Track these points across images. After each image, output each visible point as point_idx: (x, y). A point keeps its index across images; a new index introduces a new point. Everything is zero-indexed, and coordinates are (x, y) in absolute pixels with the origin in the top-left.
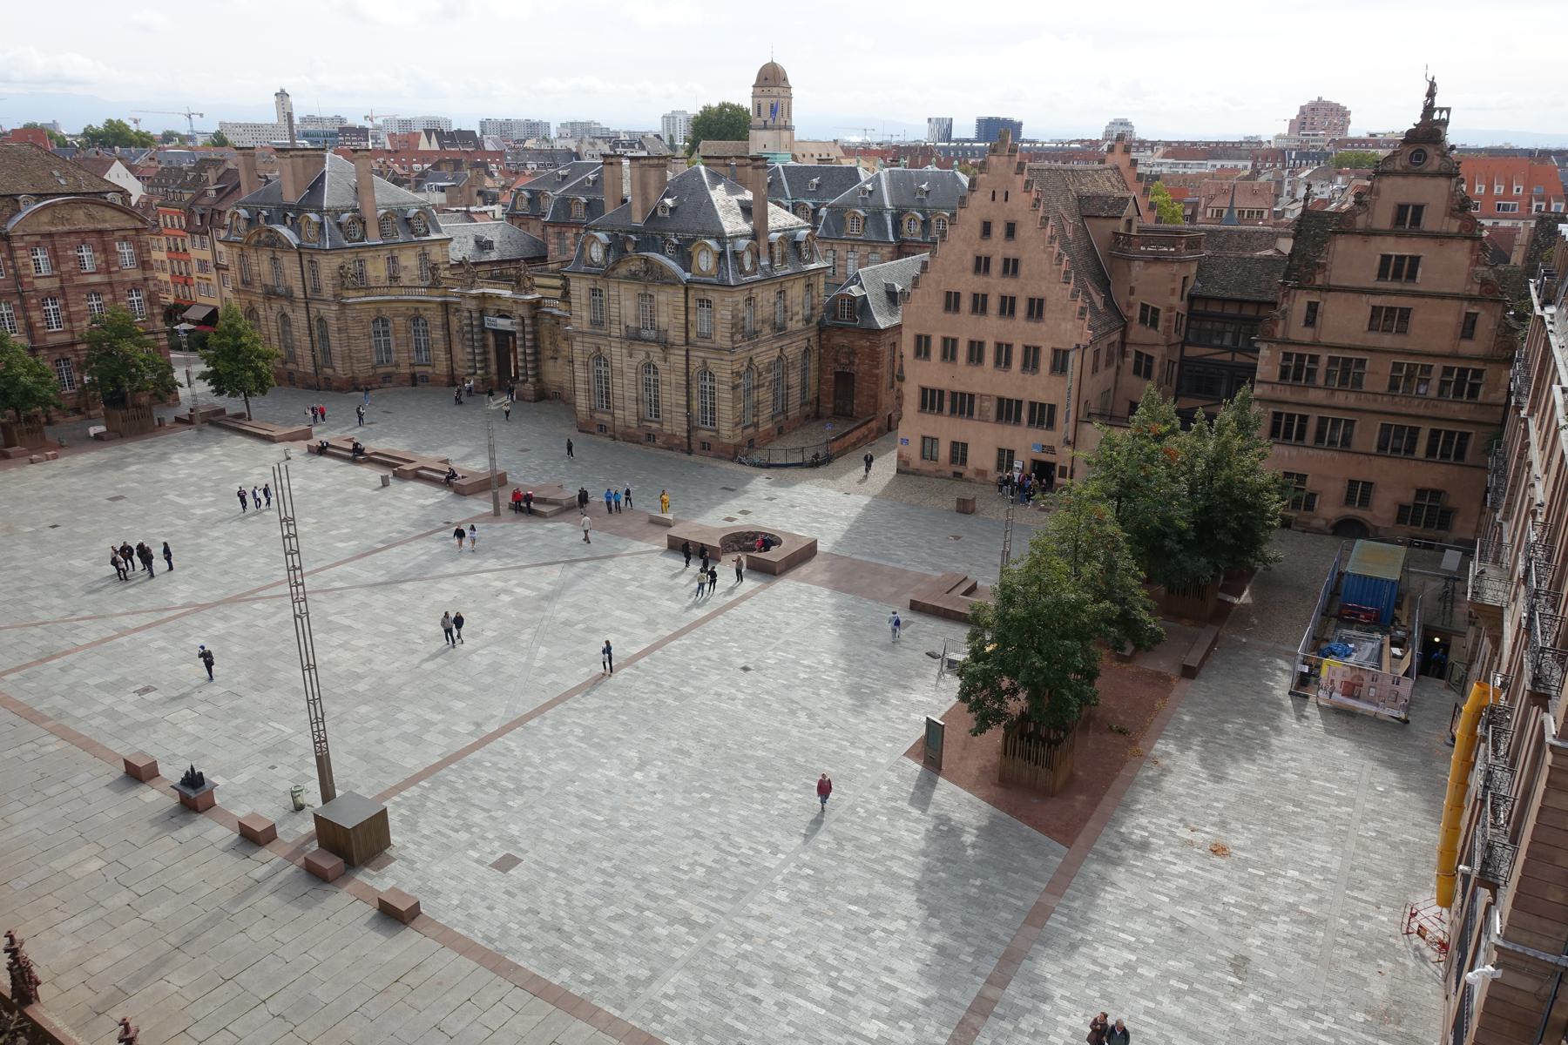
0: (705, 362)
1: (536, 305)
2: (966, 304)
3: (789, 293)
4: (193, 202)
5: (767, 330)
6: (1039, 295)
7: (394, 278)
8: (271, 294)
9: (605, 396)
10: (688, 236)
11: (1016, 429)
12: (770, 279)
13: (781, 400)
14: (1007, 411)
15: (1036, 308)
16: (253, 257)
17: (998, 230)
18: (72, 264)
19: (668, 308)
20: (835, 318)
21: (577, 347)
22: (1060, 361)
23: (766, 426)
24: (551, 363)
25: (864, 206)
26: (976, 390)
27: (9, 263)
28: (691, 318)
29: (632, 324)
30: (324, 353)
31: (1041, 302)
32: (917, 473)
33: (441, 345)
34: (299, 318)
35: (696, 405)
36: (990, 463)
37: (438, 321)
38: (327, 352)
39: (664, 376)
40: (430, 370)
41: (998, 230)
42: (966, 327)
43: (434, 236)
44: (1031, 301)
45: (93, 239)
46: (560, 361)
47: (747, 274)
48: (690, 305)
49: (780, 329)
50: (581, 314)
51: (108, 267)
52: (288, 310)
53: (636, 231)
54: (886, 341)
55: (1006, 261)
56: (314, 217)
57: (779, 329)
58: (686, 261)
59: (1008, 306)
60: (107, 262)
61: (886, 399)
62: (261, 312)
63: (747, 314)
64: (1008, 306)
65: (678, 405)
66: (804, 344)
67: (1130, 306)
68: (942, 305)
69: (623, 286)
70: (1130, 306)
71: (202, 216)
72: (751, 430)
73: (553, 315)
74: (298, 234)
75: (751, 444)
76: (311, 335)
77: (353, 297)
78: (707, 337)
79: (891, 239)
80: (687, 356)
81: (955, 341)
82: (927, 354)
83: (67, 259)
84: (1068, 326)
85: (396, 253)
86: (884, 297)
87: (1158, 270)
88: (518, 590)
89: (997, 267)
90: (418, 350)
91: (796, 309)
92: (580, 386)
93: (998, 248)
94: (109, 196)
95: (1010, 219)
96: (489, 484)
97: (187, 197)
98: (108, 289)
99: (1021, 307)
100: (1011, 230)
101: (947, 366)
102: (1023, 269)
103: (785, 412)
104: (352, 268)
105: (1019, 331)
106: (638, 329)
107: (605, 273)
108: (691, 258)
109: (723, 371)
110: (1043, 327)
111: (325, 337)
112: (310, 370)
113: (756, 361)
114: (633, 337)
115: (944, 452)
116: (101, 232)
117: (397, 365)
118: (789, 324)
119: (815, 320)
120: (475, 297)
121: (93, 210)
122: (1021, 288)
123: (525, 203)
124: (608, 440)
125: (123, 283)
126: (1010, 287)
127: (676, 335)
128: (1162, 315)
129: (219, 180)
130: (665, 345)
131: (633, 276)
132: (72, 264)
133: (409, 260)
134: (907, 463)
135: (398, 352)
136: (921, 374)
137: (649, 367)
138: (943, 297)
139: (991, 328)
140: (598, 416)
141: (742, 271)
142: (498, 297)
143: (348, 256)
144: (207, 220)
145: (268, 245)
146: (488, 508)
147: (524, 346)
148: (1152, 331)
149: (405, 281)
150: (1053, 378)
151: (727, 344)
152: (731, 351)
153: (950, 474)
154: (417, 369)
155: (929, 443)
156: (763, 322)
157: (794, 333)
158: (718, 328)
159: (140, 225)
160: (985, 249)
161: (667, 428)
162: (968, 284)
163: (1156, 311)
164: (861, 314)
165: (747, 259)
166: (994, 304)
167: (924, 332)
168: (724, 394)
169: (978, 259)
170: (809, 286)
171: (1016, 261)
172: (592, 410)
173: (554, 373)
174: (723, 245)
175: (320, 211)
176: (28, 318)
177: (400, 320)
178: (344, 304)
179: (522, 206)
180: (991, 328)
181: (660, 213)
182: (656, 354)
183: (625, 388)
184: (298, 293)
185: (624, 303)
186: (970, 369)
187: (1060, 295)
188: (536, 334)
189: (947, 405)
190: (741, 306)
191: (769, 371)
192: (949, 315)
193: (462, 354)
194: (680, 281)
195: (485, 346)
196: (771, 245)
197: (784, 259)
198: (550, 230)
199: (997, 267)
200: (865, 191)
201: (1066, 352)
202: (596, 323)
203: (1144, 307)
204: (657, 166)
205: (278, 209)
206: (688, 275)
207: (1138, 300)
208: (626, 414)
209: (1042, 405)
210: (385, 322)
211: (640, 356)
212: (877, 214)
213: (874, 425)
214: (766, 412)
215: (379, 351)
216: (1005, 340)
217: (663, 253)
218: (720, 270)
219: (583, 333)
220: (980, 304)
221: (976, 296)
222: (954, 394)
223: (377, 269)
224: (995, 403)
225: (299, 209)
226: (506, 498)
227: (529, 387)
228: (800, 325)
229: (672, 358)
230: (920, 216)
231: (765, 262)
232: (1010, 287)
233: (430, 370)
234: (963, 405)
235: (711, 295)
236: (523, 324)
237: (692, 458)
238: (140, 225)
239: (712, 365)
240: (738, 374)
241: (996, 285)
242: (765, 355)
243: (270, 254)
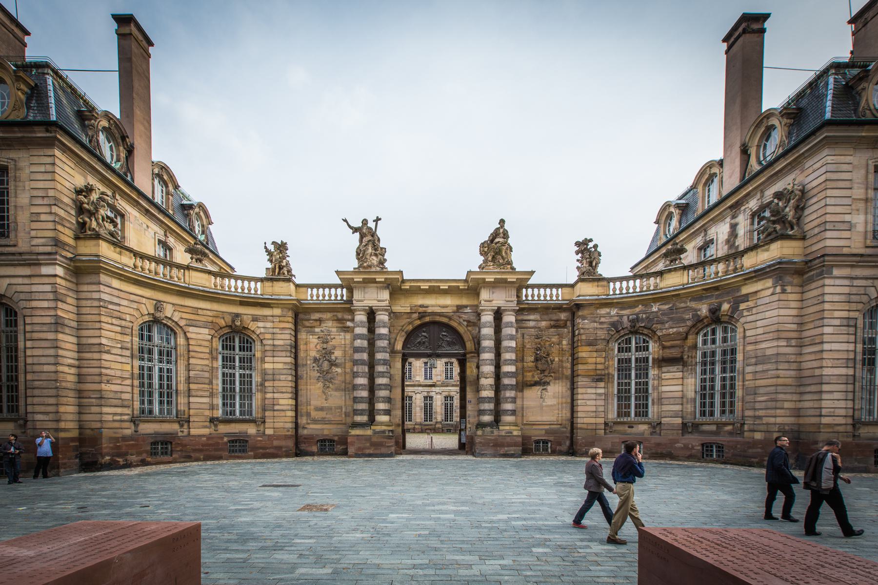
33: (286, 382)
37: (284, 338)
210: (170, 330)
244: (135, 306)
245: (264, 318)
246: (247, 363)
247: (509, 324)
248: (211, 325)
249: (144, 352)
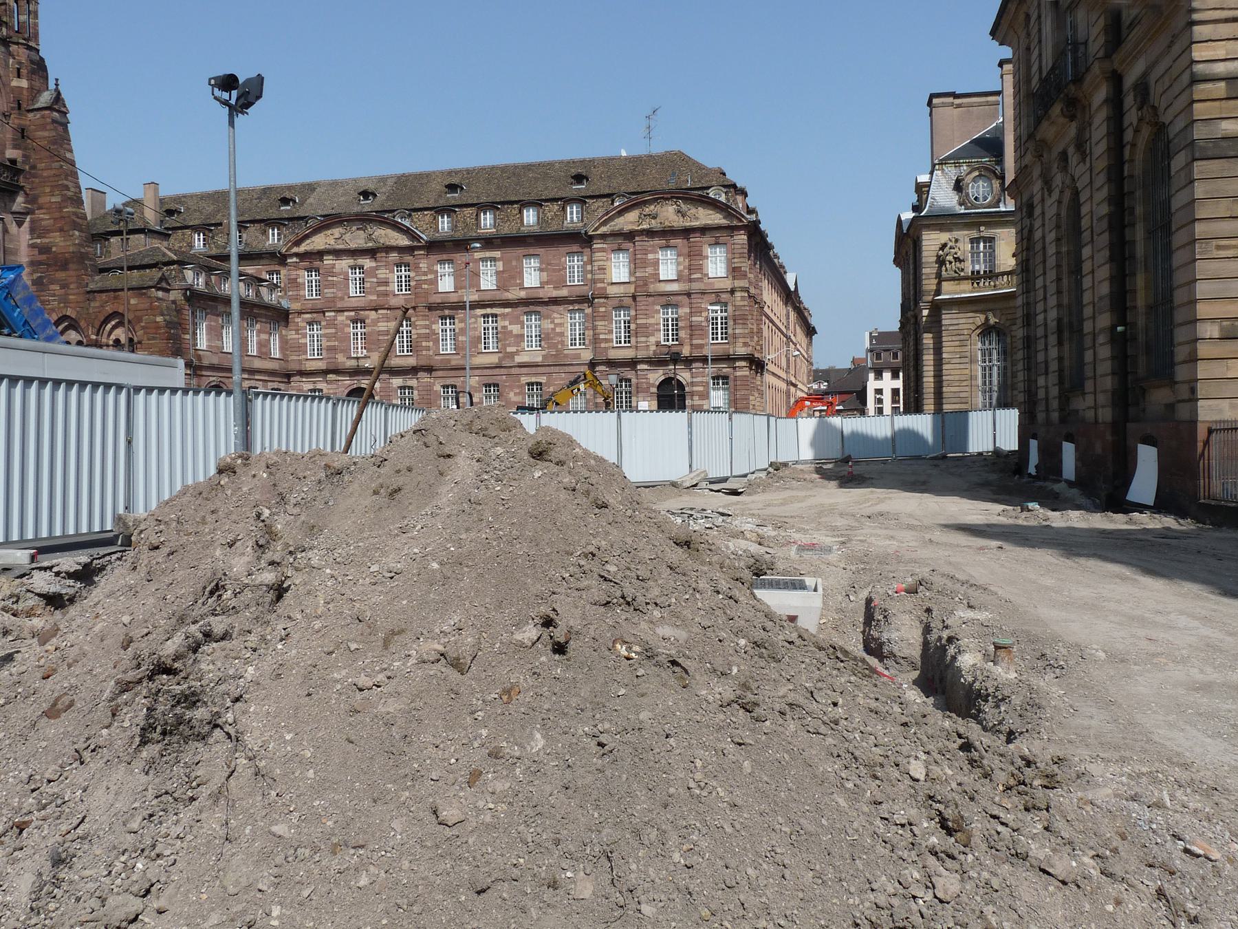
27: (589, 268)
45: (678, 242)
60: (690, 269)
98: (685, 299)
116: (686, 232)
176: (594, 328)
238: (735, 223)
244: (971, 321)
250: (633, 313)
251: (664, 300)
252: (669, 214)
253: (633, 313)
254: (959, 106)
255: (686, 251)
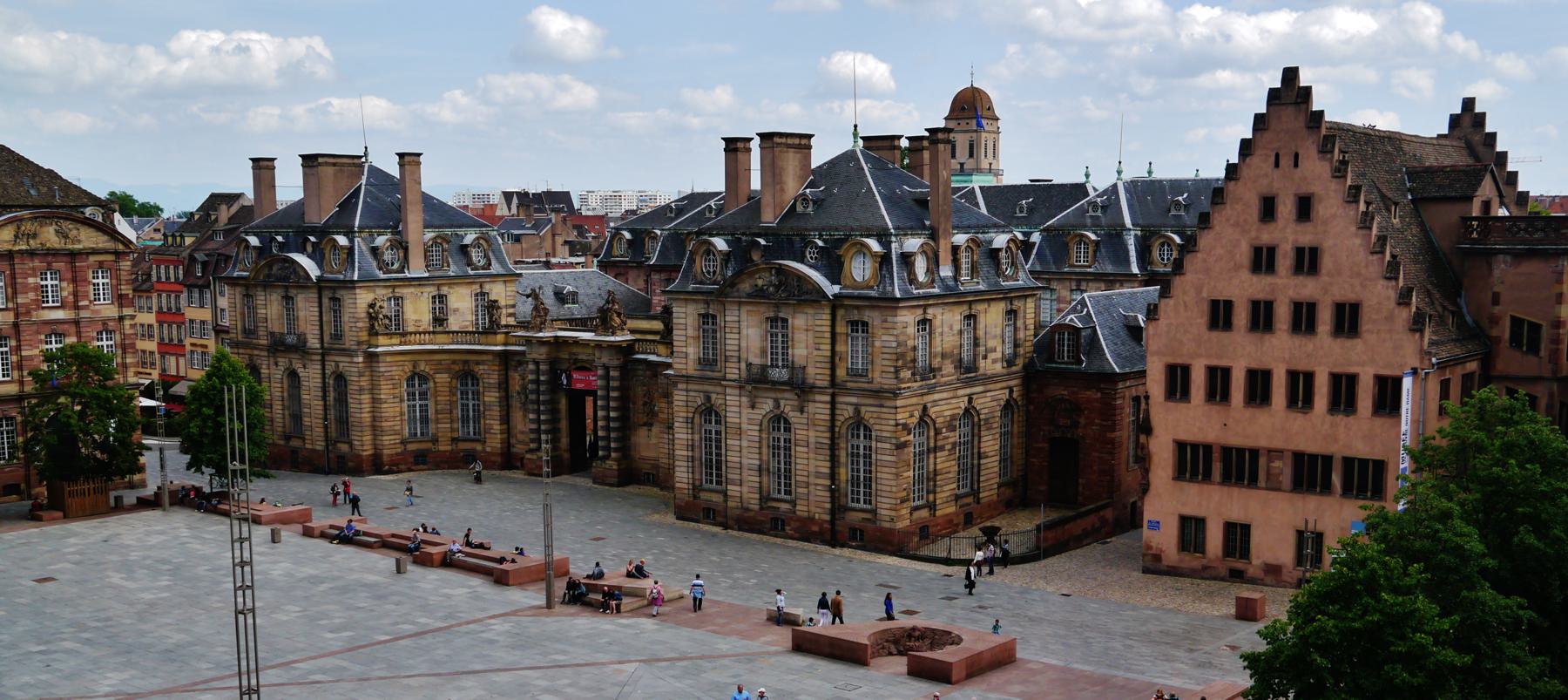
0: (857, 411)
1: (627, 350)
2: (1241, 317)
3: (982, 320)
4: (197, 247)
5: (949, 368)
6: (1350, 296)
7: (439, 320)
8: (278, 346)
9: (713, 464)
10: (838, 234)
11: (1327, 501)
12: (952, 295)
13: (970, 470)
14: (1310, 473)
15: (1348, 320)
16: (260, 298)
17: (1286, 208)
18: (31, 295)
19: (808, 339)
20: (1051, 359)
21: (679, 397)
22: (1387, 397)
23: (946, 509)
24: (643, 431)
25: (1095, 226)
26: (1262, 443)
28: (839, 348)
29: (756, 361)
30: (342, 422)
31: (1355, 308)
32: (1173, 572)
33: (496, 412)
34: (311, 376)
35: (844, 474)
36: (1285, 555)
37: (494, 379)
38: (344, 422)
39: (800, 434)
40: (479, 447)
41: (1286, 208)
42: (1241, 351)
43: (496, 268)
44: (1340, 308)
45: (60, 265)
46: (655, 429)
47: (920, 286)
48: (838, 330)
49: (968, 370)
50: (687, 352)
51: (76, 301)
52: (297, 366)
53: (765, 233)
54: (1126, 391)
55: (1300, 251)
56: (342, 240)
57: (968, 370)
58: (835, 271)
59: (1304, 318)
60: (75, 294)
61: (1129, 478)
62: (264, 371)
63: (919, 342)
64: (1304, 318)
65: (818, 475)
66: (1004, 395)
67: (1494, 320)
68: (1201, 320)
69: (744, 309)
70: (1494, 320)
71: (205, 265)
72: (924, 513)
73: (645, 361)
74: (320, 266)
75: (925, 532)
76: (324, 398)
77: (384, 345)
78: (864, 374)
79: (1135, 270)
80: (833, 404)
81: (1226, 372)
82: (1185, 395)
83: (27, 288)
84: (1391, 345)
85: (445, 290)
86: (1123, 333)
87: (1531, 267)
88: (569, 690)
89: (1284, 262)
90: (465, 420)
91: (991, 344)
92: (681, 452)
93: (1286, 234)
94: (88, 211)
95: (1304, 190)
96: (546, 573)
97: (188, 241)
98: (73, 329)
99: (1325, 318)
100: (1305, 208)
101: (1215, 410)
102: (1327, 262)
103: (975, 493)
104: (388, 308)
105: (1324, 354)
106: (764, 368)
107: (720, 295)
108: (841, 265)
109: (883, 422)
110: (1357, 344)
111: (342, 400)
112: (320, 445)
113: (932, 411)
114: (757, 381)
115: (1214, 539)
116: (73, 255)
117: (435, 441)
118: (982, 363)
119: (1020, 362)
120: (541, 342)
121: (67, 226)
122: (1323, 291)
123: (624, 246)
124: (718, 529)
125: (91, 321)
126: (1307, 288)
127: (817, 374)
128: (1546, 332)
129: (231, 220)
130: (801, 388)
131: (759, 295)
132: (31, 295)
133: (462, 303)
134: (1157, 558)
135: (437, 421)
136: (1175, 423)
137: (779, 420)
138: (1206, 307)
139: (1280, 351)
140: (704, 496)
141: (912, 279)
142: (576, 342)
143: (384, 291)
144: (211, 268)
145: (279, 279)
146: (542, 601)
147: (607, 408)
148: (1532, 359)
149: (454, 323)
150: (1379, 421)
151: (889, 382)
152: (895, 394)
153: (1224, 572)
154: (462, 446)
155: (1191, 529)
156: (943, 356)
157: (989, 379)
158: (878, 361)
159: (121, 247)
160: (1267, 236)
161: (801, 509)
162: (1243, 288)
163: (1535, 328)
164: (1088, 355)
165: (920, 266)
166: (1283, 314)
167: (1179, 361)
168: (884, 454)
169: (1258, 251)
170: (1012, 314)
171: (1314, 252)
172: (696, 488)
173: (647, 444)
174: (886, 245)
175: (349, 233)
177: (442, 378)
178: (376, 355)
179: (620, 252)
180: (1280, 351)
181: (800, 208)
182: (788, 406)
183: (744, 452)
184: (313, 342)
185: (746, 334)
186: (1249, 412)
187: (1378, 296)
188: (625, 389)
189: (1217, 468)
190: (911, 330)
191: (952, 428)
192: (1215, 335)
193: (522, 423)
194: (825, 295)
195: (554, 412)
196: (955, 249)
197: (974, 270)
198: (655, 277)
199: (1284, 262)
200: (1094, 205)
201: (1397, 381)
202: (706, 362)
203: (1517, 322)
204: (799, 147)
205: (297, 233)
206: (836, 289)
207: (1505, 311)
208: (744, 489)
209: (1364, 463)
210: (424, 378)
211: (767, 406)
212: (1114, 236)
213: (1109, 514)
214: (947, 490)
215: (412, 420)
216: (1302, 366)
217: (802, 262)
218: (883, 277)
219: (688, 379)
220: (1262, 316)
221: (1255, 304)
222: (1227, 451)
223: (417, 310)
224: (1289, 460)
225: (324, 232)
226: (560, 587)
227: (612, 464)
228: (998, 368)
229: (811, 407)
230: (1177, 239)
231: (946, 271)
232: (1307, 288)
233: (479, 447)
234: (1240, 466)
235: (867, 316)
236: (607, 377)
237: (837, 551)
239: (868, 413)
240: (905, 426)
241: (1285, 288)
242: (946, 405)
243: (281, 292)
245: (483, 363)
246: (477, 395)
247: (614, 379)
248: (448, 370)
249: (411, 395)
250: (13, 343)
251: (48, 330)
252: (49, 236)
253: (13, 343)
254: (334, 165)
255: (69, 275)
